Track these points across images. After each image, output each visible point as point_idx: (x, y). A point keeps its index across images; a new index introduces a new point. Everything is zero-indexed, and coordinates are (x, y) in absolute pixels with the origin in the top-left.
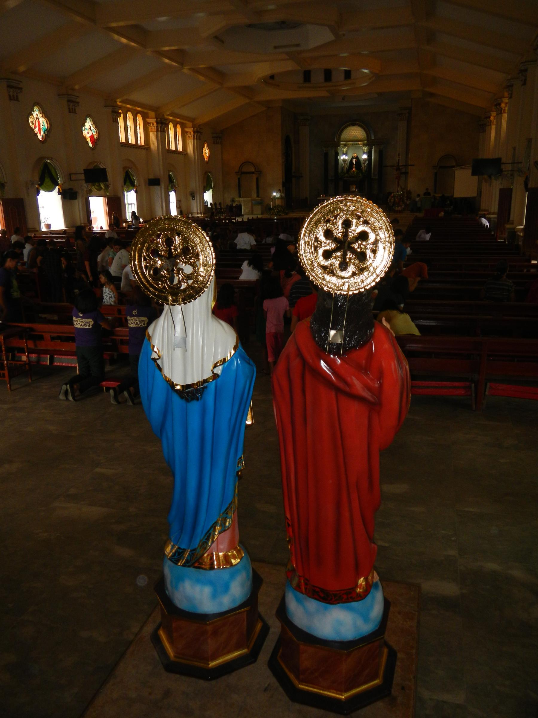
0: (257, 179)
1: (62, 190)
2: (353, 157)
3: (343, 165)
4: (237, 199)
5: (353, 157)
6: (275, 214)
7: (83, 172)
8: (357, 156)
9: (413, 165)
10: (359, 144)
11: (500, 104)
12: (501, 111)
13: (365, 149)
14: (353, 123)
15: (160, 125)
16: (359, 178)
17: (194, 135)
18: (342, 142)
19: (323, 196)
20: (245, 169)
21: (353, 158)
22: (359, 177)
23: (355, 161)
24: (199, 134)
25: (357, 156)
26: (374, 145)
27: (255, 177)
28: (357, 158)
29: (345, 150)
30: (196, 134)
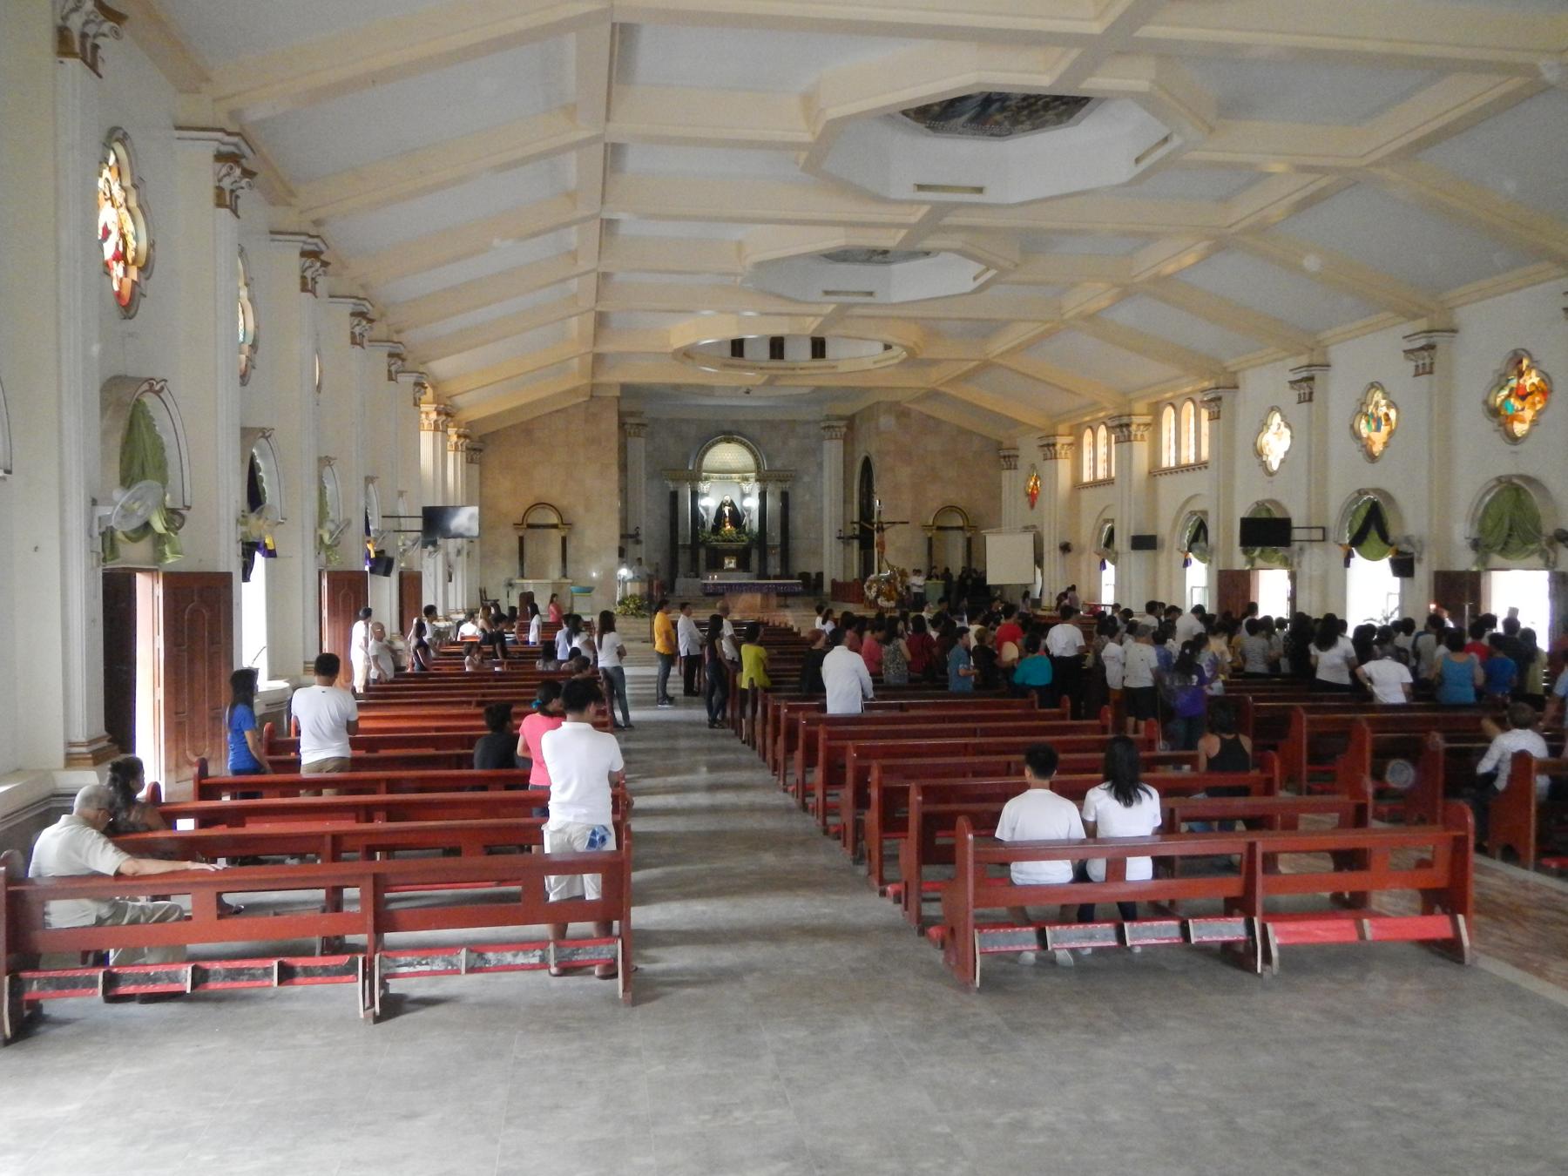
0: (564, 540)
1: (376, 553)
4: (518, 581)
6: (632, 614)
7: (420, 514)
9: (907, 523)
11: (1128, 425)
12: (1129, 436)
14: (729, 436)
15: (444, 418)
17: (456, 443)
18: (706, 471)
19: (713, 578)
20: (535, 518)
21: (723, 505)
24: (468, 441)
27: (556, 536)
28: (732, 504)
30: (462, 440)
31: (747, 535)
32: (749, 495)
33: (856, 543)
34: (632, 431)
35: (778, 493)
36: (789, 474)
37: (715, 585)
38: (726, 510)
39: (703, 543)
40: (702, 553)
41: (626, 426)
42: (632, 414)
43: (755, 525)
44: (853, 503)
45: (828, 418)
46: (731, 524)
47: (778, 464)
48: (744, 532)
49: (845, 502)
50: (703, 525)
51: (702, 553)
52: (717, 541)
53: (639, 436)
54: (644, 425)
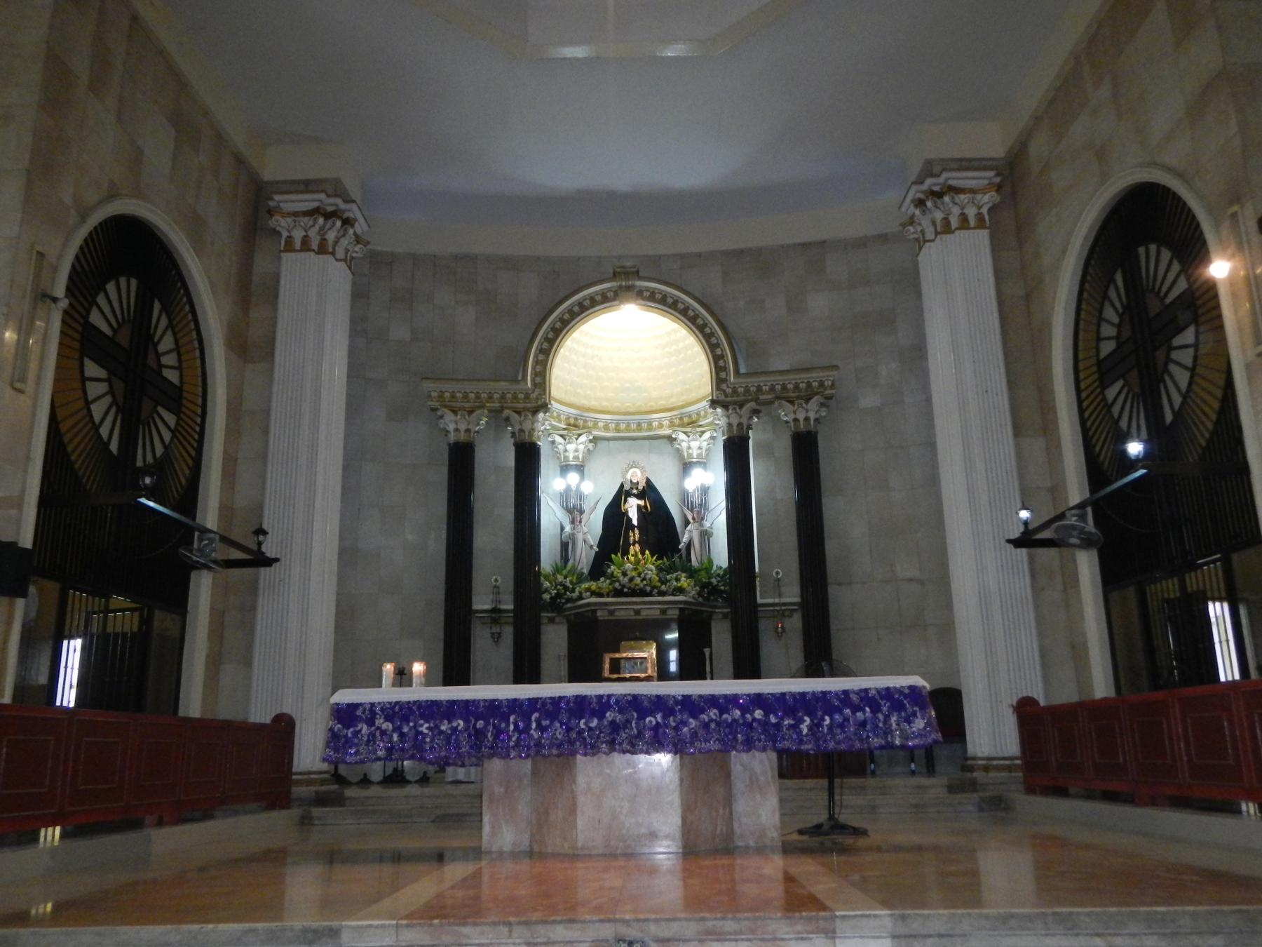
2: (622, 486)
3: (568, 528)
5: (627, 487)
8: (648, 482)
10: (655, 424)
13: (695, 444)
16: (681, 598)
19: (403, 676)
21: (622, 494)
22: (680, 590)
23: (639, 506)
25: (648, 482)
26: (756, 412)
28: (649, 492)
29: (576, 451)
31: (692, 573)
32: (703, 464)
33: (1087, 565)
34: (298, 235)
35: (784, 447)
36: (815, 377)
37: (399, 713)
38: (632, 507)
39: (556, 605)
40: (555, 639)
41: (282, 224)
42: (307, 186)
44: (1048, 428)
45: (929, 170)
46: (644, 544)
47: (779, 362)
49: (1018, 430)
51: (555, 639)
52: (594, 593)
53: (322, 249)
54: (329, 216)
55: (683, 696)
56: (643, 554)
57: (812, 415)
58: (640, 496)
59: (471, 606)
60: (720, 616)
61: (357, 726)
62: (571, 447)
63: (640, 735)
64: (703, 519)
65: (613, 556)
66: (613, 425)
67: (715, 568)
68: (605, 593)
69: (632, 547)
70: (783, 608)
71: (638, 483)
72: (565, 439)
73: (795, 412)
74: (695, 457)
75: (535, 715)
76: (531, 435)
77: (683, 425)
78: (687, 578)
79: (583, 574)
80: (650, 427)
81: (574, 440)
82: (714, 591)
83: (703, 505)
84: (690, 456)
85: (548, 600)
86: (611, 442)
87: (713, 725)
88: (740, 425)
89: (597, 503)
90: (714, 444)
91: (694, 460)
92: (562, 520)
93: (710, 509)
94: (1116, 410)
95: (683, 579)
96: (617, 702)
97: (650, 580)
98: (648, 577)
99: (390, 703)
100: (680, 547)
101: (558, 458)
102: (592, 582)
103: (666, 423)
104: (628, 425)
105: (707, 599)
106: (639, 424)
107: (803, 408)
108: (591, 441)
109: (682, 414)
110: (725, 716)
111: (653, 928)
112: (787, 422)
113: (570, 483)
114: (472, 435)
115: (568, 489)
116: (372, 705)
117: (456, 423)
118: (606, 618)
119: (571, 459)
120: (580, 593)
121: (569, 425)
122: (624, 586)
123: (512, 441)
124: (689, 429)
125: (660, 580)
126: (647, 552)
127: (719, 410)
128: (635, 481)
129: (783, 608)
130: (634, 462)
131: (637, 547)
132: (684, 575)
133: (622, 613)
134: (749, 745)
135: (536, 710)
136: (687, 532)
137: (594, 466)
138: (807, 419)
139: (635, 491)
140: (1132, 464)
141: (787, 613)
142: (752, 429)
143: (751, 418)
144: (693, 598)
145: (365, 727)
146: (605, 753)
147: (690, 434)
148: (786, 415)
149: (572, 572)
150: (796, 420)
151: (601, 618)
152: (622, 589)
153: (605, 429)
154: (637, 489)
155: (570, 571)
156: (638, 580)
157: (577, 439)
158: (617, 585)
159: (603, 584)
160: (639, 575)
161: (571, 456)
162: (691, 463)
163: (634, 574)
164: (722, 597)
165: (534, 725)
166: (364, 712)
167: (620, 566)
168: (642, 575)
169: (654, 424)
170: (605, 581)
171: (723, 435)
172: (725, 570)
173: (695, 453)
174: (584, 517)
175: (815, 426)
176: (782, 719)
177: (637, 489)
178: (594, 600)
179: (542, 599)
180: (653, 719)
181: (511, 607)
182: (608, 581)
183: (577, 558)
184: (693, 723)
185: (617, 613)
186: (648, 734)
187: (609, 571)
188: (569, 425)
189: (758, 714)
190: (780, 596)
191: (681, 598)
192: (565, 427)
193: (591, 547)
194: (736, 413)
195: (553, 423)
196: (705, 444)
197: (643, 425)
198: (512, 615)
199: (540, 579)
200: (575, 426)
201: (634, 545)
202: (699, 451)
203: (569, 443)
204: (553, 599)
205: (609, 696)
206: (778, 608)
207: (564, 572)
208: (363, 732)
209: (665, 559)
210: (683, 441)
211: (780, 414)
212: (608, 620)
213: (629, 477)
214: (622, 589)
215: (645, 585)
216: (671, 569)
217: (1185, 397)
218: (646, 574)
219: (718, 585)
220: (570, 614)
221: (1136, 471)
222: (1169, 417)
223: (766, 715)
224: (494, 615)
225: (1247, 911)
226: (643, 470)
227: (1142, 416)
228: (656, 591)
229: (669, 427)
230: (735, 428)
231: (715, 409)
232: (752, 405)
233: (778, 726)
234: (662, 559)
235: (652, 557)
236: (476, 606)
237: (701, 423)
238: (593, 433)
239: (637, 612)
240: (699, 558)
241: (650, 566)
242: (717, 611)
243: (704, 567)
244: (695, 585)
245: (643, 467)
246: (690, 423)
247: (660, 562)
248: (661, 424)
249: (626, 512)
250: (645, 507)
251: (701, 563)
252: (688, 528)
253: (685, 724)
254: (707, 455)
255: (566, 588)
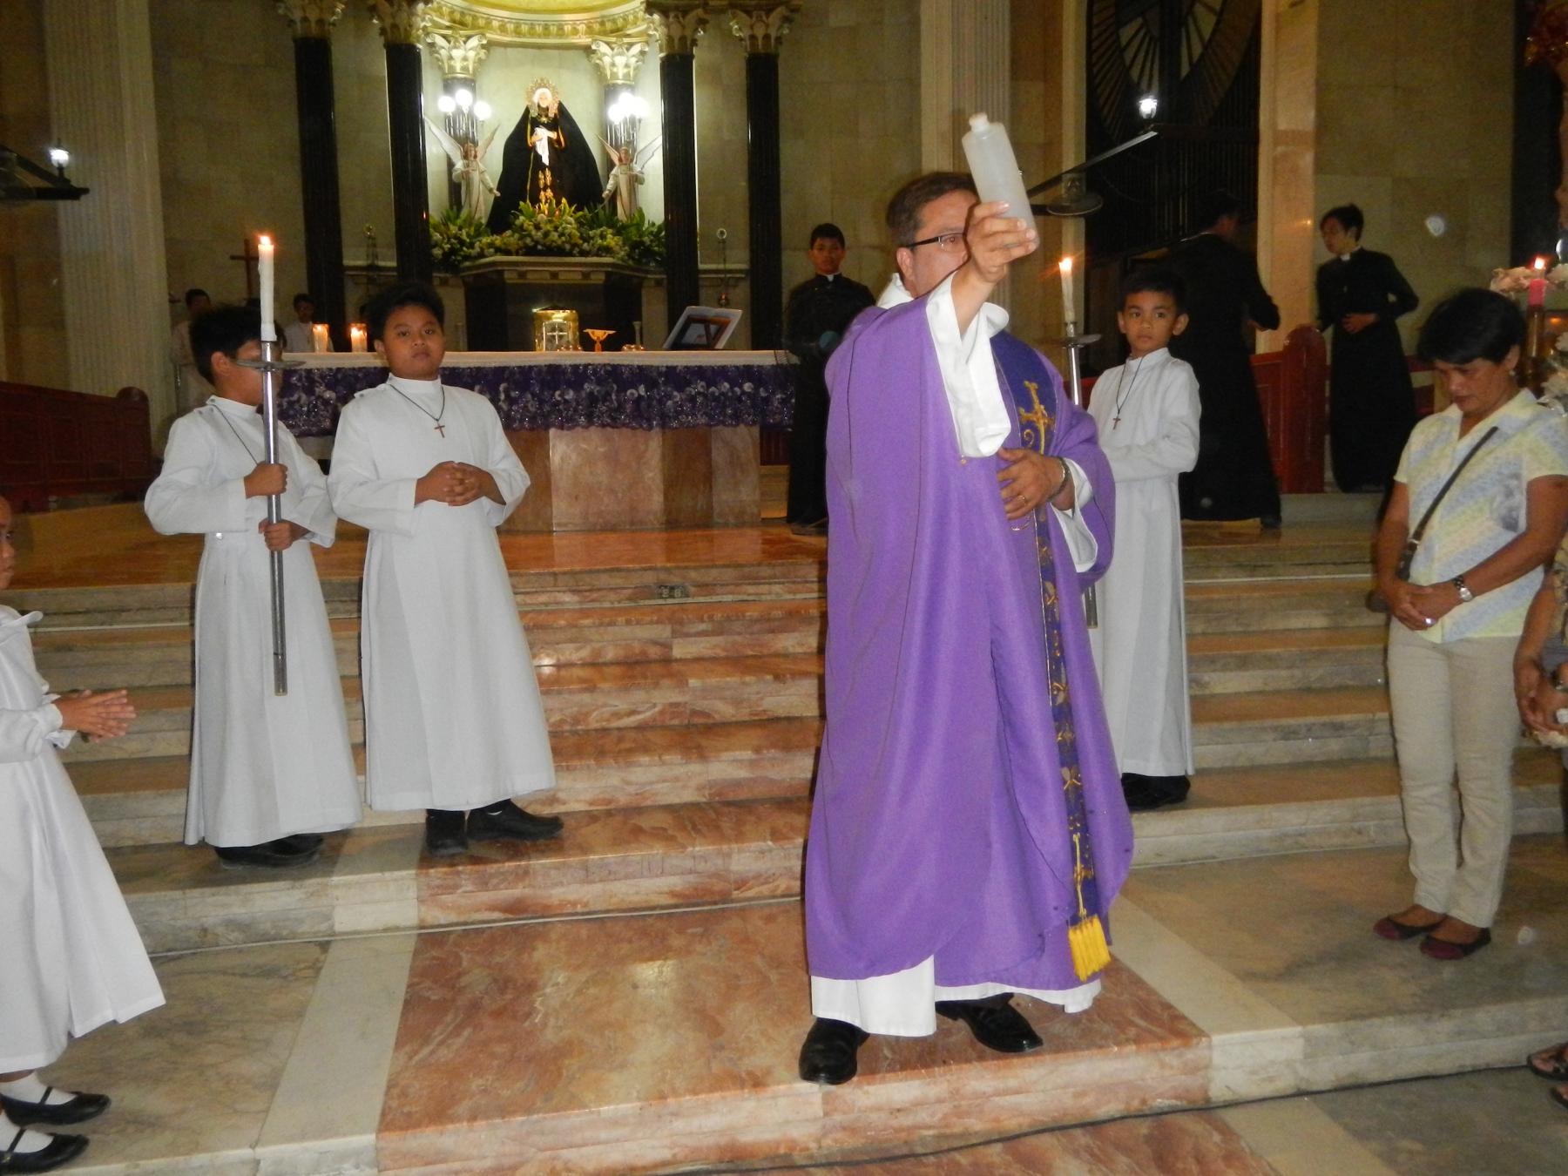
2: (527, 111)
3: (459, 165)
5: (534, 113)
10: (567, 28)
13: (620, 60)
16: (607, 260)
19: (340, 342)
21: (527, 123)
22: (607, 250)
23: (550, 140)
25: (561, 108)
26: (702, 22)
28: (561, 120)
29: (465, 59)
31: (620, 230)
35: (736, 72)
38: (542, 140)
39: (450, 262)
43: (653, 203)
48: (611, 221)
49: (1018, 69)
50: (456, 190)
52: (498, 250)
55: (667, 367)
56: (558, 203)
57: (773, 33)
58: (552, 126)
59: (342, 260)
60: (653, 283)
61: (292, 396)
62: (455, 53)
63: (620, 408)
64: (632, 161)
65: (522, 203)
66: (512, 26)
67: (646, 225)
68: (513, 250)
69: (542, 193)
70: (728, 275)
71: (547, 109)
72: (449, 42)
73: (752, 27)
74: (621, 77)
75: (502, 387)
76: (408, 34)
77: (605, 33)
78: (614, 235)
79: (481, 224)
80: (561, 31)
81: (462, 40)
82: (647, 252)
83: (630, 143)
84: (614, 75)
85: (440, 257)
86: (509, 50)
87: (699, 400)
88: (683, 39)
89: (494, 133)
90: (643, 61)
91: (620, 82)
92: (451, 154)
93: (638, 150)
94: (1128, 56)
95: (609, 236)
96: (595, 372)
97: (570, 235)
98: (567, 231)
99: (331, 369)
100: (604, 195)
101: (441, 68)
102: (495, 236)
103: (582, 28)
104: (532, 27)
105: (638, 261)
106: (546, 27)
107: (764, 22)
108: (483, 47)
109: (603, 17)
110: (712, 389)
111: (693, 574)
112: (741, 39)
113: (461, 103)
114: (326, 27)
115: (459, 111)
116: (309, 372)
117: (304, 11)
118: (515, 281)
119: (458, 70)
120: (482, 249)
121: (454, 22)
122: (537, 243)
123: (381, 41)
124: (614, 39)
125: (581, 237)
126: (564, 200)
127: (656, 17)
128: (544, 106)
129: (728, 275)
130: (542, 80)
131: (549, 193)
132: (610, 231)
133: (536, 276)
134: (737, 418)
135: (507, 380)
136: (611, 177)
137: (487, 81)
138: (767, 37)
139: (544, 119)
140: (1143, 124)
141: (731, 282)
142: (697, 45)
143: (696, 30)
144: (622, 259)
145: (304, 397)
146: (583, 427)
147: (613, 46)
148: (740, 29)
149: (469, 221)
150: (753, 37)
151: (508, 281)
152: (535, 246)
153: (502, 31)
154: (547, 116)
155: (465, 221)
156: (555, 236)
157: (465, 42)
158: (528, 240)
159: (509, 238)
160: (556, 228)
161: (458, 65)
162: (615, 85)
163: (549, 227)
164: (657, 261)
165: (502, 397)
166: (300, 380)
167: (531, 217)
168: (560, 229)
169: (566, 27)
170: (513, 236)
171: (661, 51)
172: (659, 227)
173: (621, 71)
174: (480, 150)
175: (776, 48)
176: (774, 393)
177: (547, 116)
178: (499, 258)
179: (431, 255)
180: (634, 391)
181: (393, 264)
182: (517, 236)
183: (474, 202)
184: (677, 396)
185: (529, 276)
186: (629, 407)
187: (517, 222)
188: (454, 22)
189: (747, 387)
190: (725, 262)
191: (607, 260)
192: (448, 24)
193: (491, 190)
194: (679, 22)
195: (436, 19)
196: (633, 60)
197: (551, 28)
198: (395, 274)
199: (428, 231)
200: (463, 24)
201: (545, 189)
202: (626, 70)
203: (455, 47)
204: (447, 255)
205: (586, 366)
206: (723, 276)
207: (459, 222)
208: (302, 402)
209: (586, 210)
210: (605, 54)
211: (731, 27)
212: (517, 284)
213: (536, 99)
214: (535, 246)
215: (563, 242)
216: (594, 223)
217: (1205, 47)
218: (564, 228)
219: (651, 245)
220: (469, 276)
221: (1146, 132)
222: (1185, 70)
223: (756, 389)
224: (371, 274)
225: (1205, 550)
226: (554, 92)
227: (1156, 67)
228: (576, 250)
229: (586, 33)
230: (676, 41)
231: (651, 14)
232: (700, 11)
233: (767, 401)
234: (582, 210)
235: (570, 206)
236: (347, 262)
237: (629, 32)
238: (488, 35)
239: (554, 275)
240: (628, 213)
241: (569, 218)
242: (649, 276)
243: (635, 222)
244: (624, 244)
245: (554, 88)
246: (614, 30)
247: (581, 213)
248: (575, 28)
249: (534, 147)
250: (558, 141)
251: (630, 217)
252: (614, 172)
253: (670, 397)
254: (635, 76)
255: (462, 242)
